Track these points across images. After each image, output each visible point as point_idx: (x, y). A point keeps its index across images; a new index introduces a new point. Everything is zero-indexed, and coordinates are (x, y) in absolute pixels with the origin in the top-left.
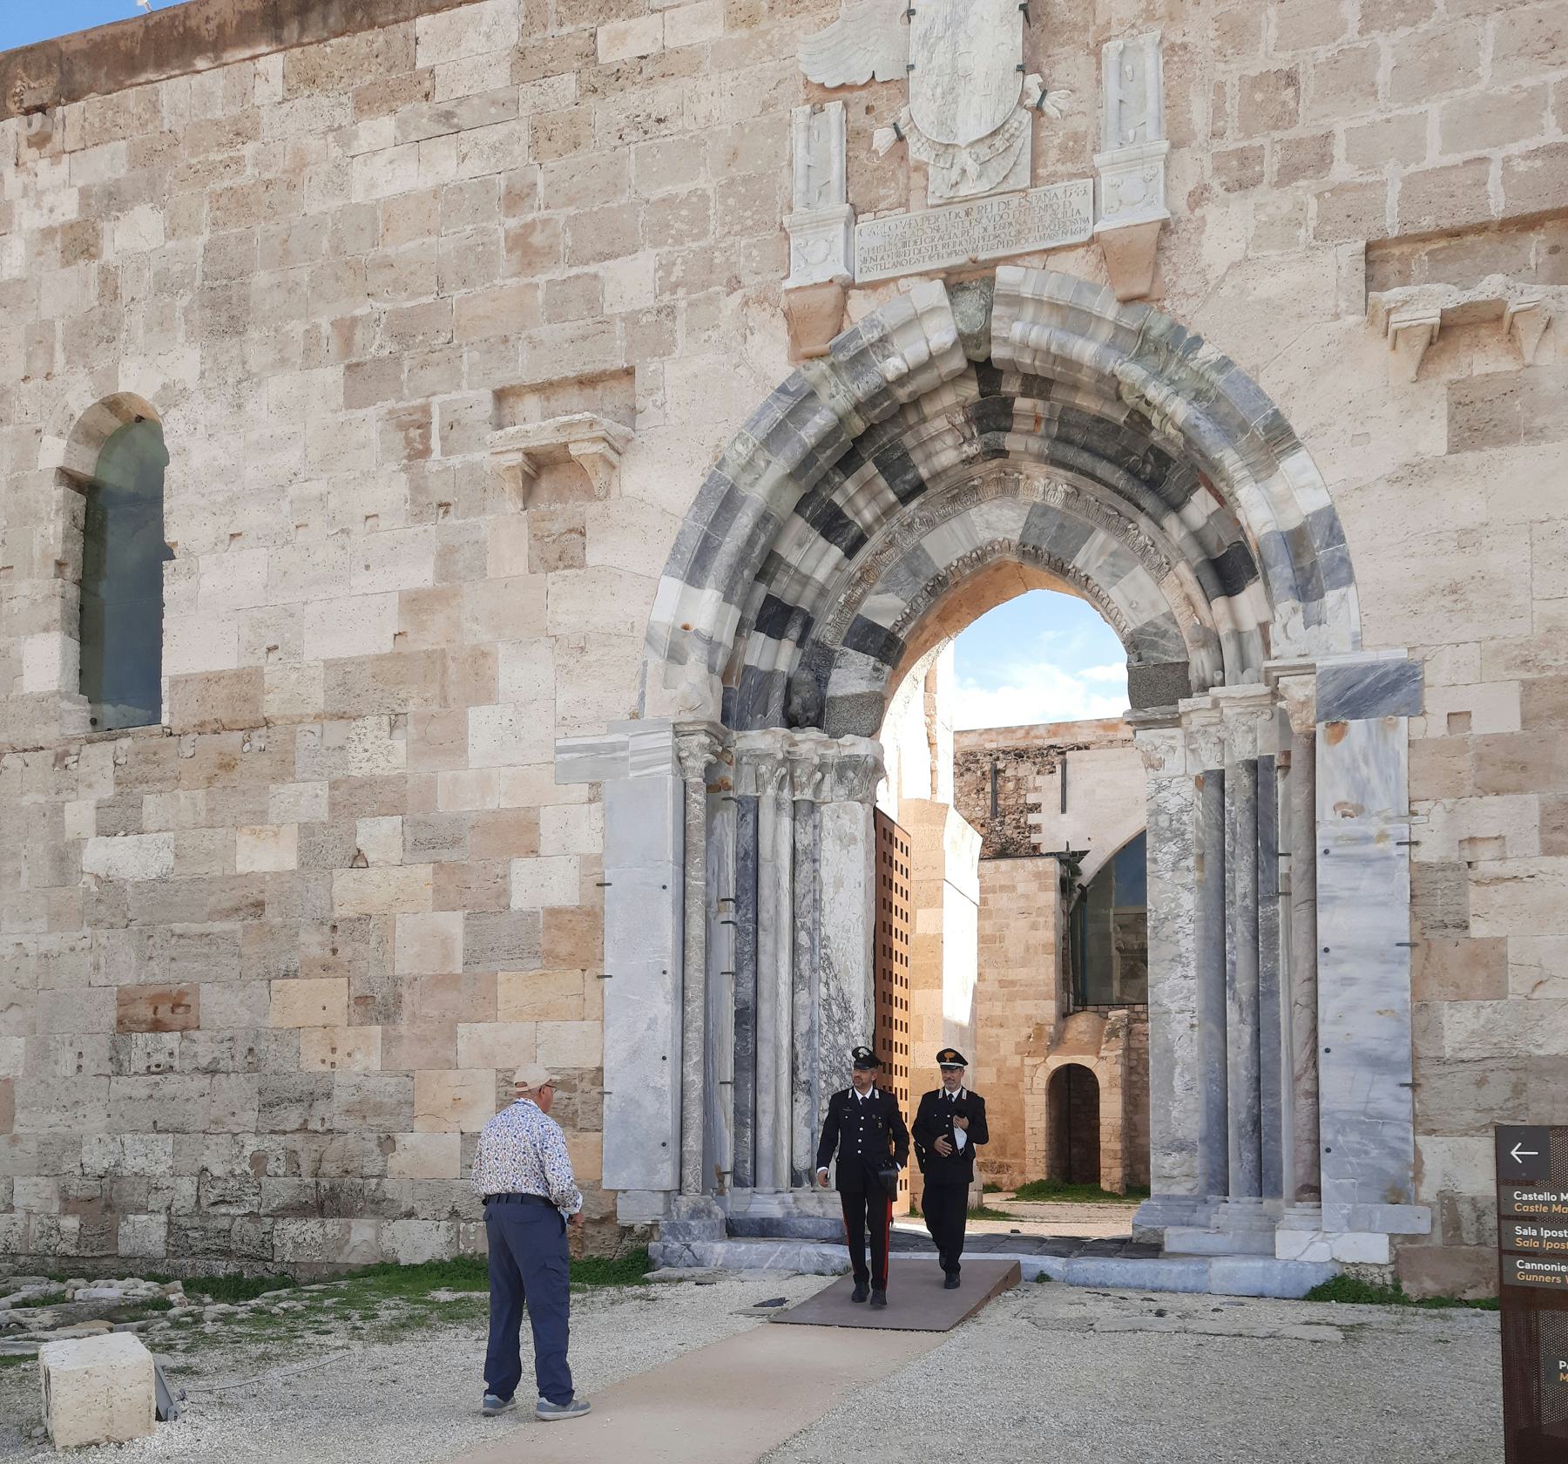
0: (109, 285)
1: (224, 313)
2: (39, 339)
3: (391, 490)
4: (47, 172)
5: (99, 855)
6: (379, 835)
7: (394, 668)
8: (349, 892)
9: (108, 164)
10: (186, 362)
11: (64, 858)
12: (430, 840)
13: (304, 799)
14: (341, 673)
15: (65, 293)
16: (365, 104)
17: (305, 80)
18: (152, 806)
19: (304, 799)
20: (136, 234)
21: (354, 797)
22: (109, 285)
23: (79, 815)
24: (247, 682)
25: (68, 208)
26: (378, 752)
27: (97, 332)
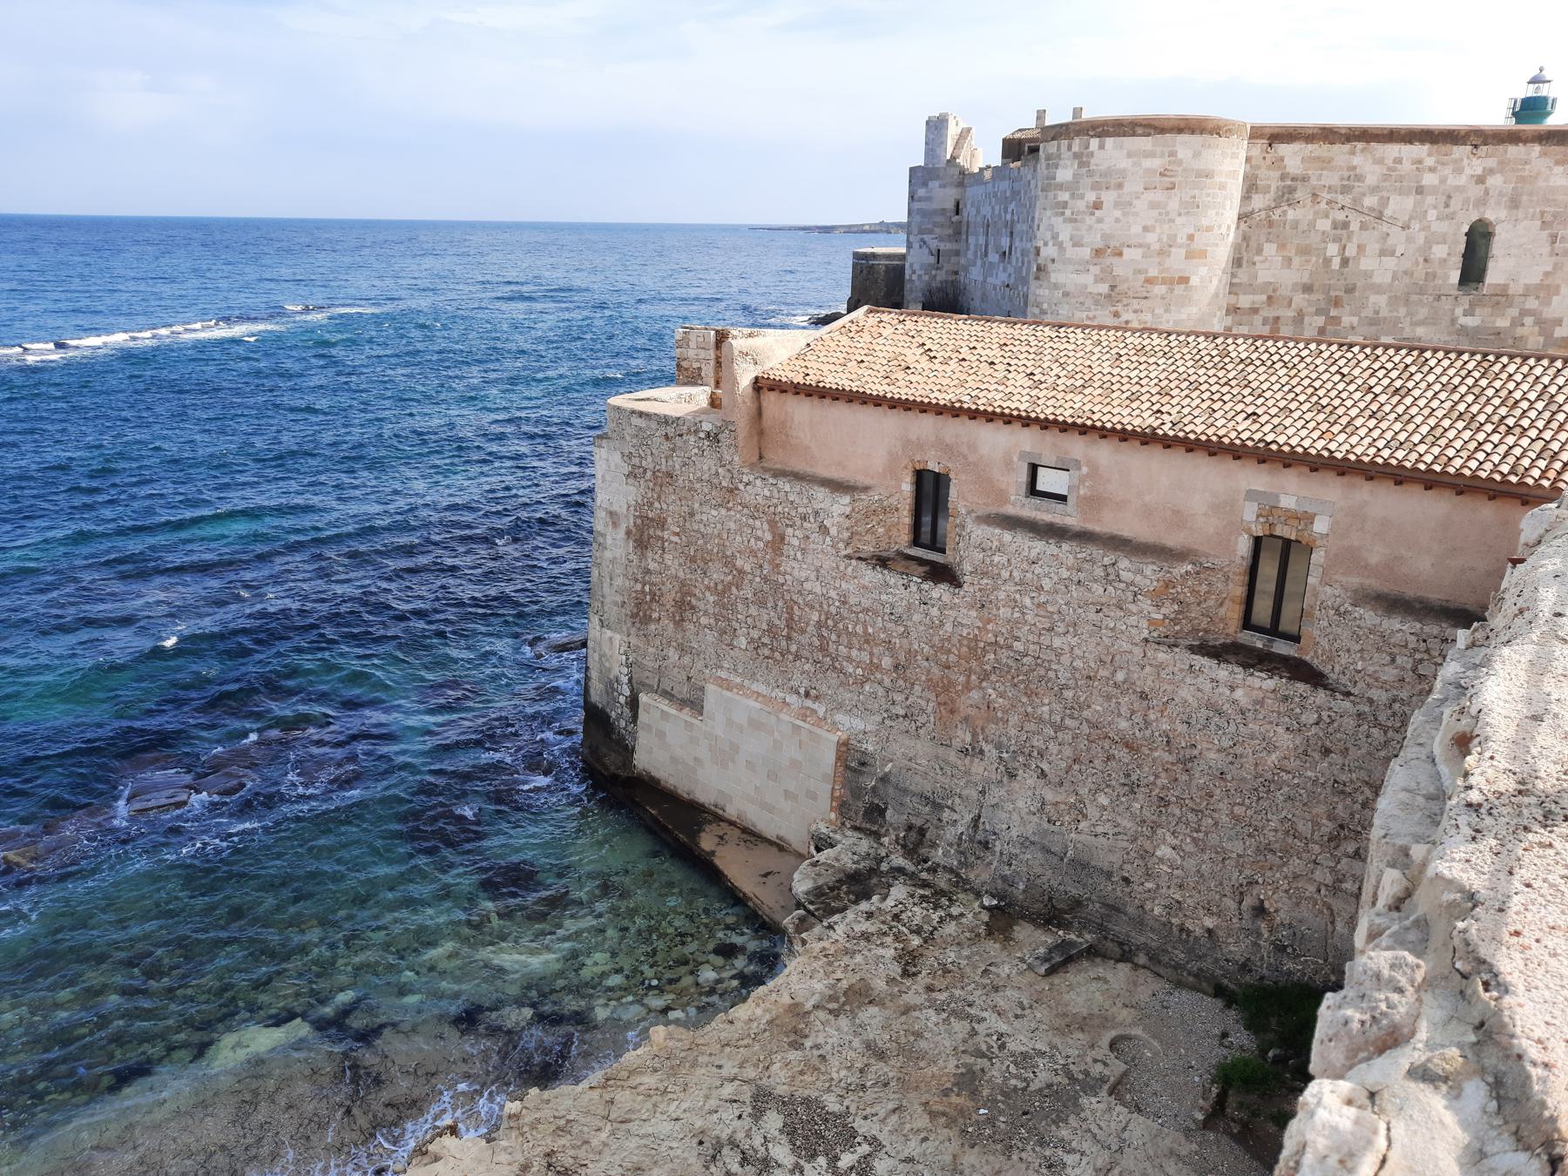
0: (1487, 192)
1: (1514, 204)
2: (1466, 201)
3: (1546, 249)
4: (1475, 161)
5: (1463, 320)
6: (1529, 320)
7: (1539, 287)
8: (1520, 331)
9: (1491, 163)
10: (1503, 214)
11: (1453, 321)
12: (1539, 322)
13: (1514, 312)
14: (1527, 287)
15: (1475, 191)
16: (1557, 163)
17: (1543, 154)
18: (1478, 311)
19: (1514, 312)
20: (1495, 181)
21: (1524, 313)
22: (1487, 192)
23: (1459, 311)
24: (1506, 287)
25: (1479, 171)
26: (1532, 304)
27: (1481, 202)
